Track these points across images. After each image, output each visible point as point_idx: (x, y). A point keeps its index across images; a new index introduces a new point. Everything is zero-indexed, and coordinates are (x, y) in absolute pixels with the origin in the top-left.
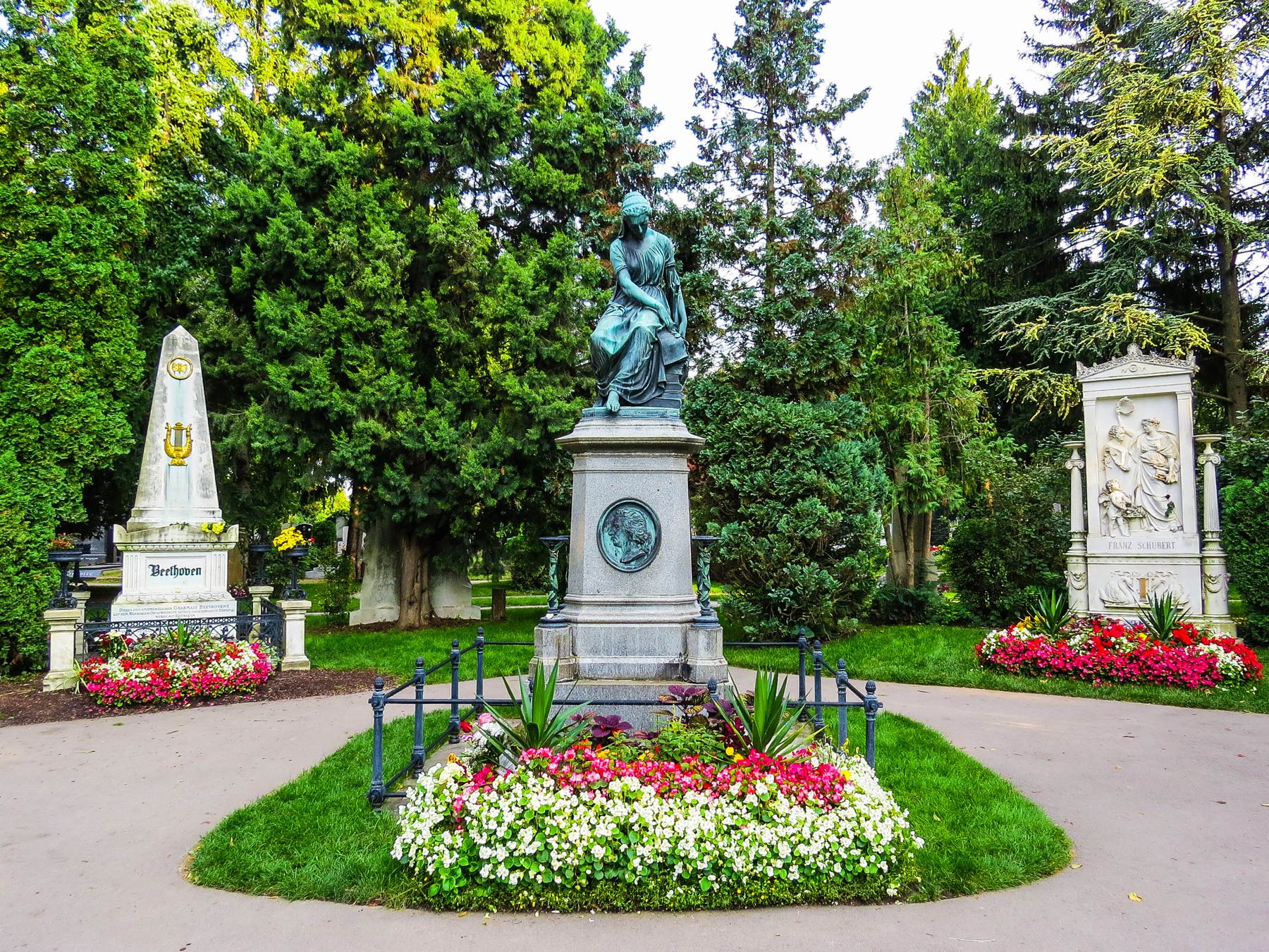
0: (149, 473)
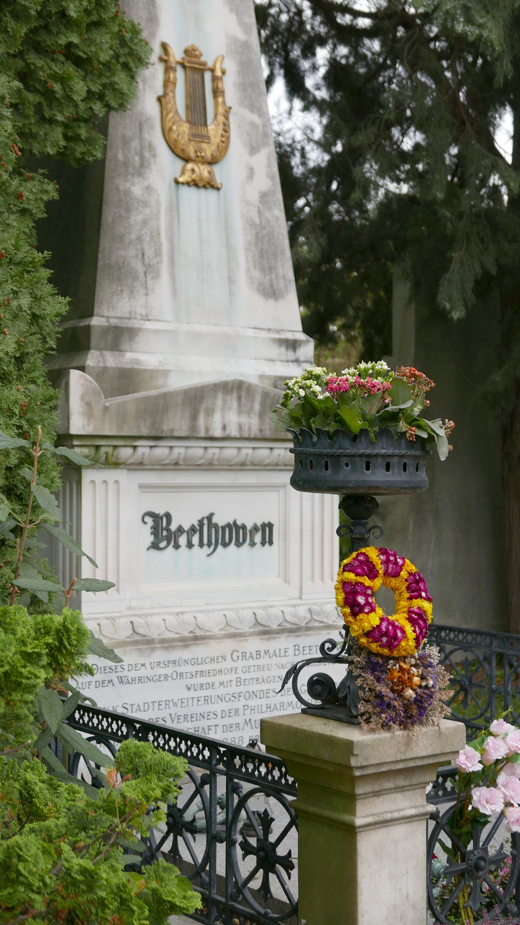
0: (127, 203)
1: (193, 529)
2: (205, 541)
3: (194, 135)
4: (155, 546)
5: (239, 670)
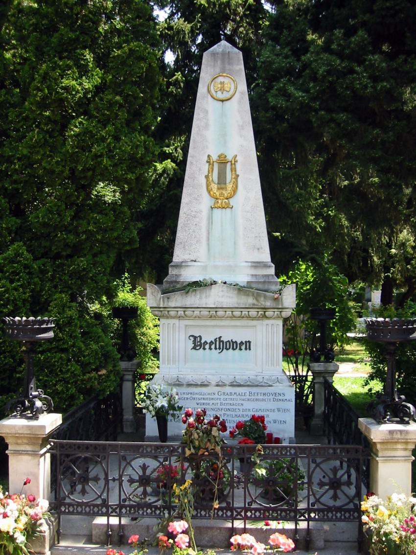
1: (211, 343)
2: (218, 347)
3: (219, 189)
4: (194, 348)
5: (222, 399)
